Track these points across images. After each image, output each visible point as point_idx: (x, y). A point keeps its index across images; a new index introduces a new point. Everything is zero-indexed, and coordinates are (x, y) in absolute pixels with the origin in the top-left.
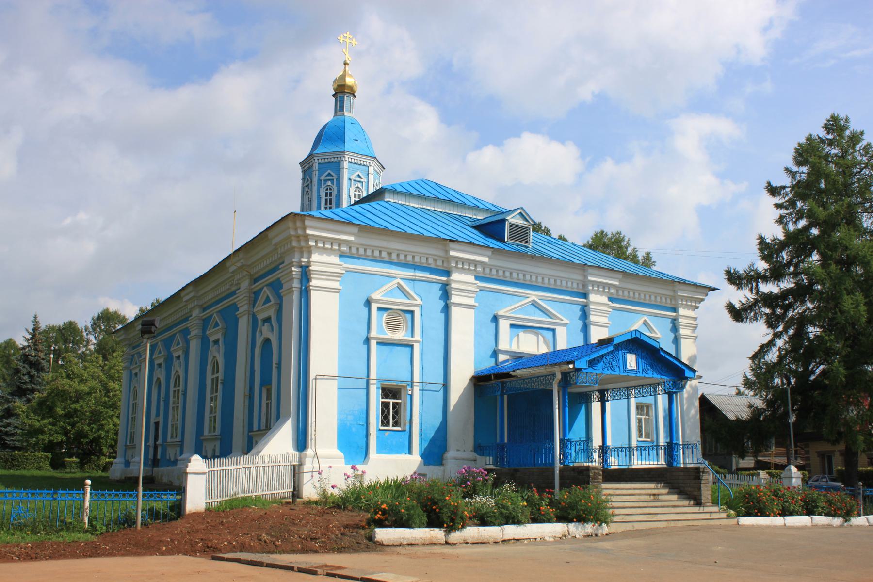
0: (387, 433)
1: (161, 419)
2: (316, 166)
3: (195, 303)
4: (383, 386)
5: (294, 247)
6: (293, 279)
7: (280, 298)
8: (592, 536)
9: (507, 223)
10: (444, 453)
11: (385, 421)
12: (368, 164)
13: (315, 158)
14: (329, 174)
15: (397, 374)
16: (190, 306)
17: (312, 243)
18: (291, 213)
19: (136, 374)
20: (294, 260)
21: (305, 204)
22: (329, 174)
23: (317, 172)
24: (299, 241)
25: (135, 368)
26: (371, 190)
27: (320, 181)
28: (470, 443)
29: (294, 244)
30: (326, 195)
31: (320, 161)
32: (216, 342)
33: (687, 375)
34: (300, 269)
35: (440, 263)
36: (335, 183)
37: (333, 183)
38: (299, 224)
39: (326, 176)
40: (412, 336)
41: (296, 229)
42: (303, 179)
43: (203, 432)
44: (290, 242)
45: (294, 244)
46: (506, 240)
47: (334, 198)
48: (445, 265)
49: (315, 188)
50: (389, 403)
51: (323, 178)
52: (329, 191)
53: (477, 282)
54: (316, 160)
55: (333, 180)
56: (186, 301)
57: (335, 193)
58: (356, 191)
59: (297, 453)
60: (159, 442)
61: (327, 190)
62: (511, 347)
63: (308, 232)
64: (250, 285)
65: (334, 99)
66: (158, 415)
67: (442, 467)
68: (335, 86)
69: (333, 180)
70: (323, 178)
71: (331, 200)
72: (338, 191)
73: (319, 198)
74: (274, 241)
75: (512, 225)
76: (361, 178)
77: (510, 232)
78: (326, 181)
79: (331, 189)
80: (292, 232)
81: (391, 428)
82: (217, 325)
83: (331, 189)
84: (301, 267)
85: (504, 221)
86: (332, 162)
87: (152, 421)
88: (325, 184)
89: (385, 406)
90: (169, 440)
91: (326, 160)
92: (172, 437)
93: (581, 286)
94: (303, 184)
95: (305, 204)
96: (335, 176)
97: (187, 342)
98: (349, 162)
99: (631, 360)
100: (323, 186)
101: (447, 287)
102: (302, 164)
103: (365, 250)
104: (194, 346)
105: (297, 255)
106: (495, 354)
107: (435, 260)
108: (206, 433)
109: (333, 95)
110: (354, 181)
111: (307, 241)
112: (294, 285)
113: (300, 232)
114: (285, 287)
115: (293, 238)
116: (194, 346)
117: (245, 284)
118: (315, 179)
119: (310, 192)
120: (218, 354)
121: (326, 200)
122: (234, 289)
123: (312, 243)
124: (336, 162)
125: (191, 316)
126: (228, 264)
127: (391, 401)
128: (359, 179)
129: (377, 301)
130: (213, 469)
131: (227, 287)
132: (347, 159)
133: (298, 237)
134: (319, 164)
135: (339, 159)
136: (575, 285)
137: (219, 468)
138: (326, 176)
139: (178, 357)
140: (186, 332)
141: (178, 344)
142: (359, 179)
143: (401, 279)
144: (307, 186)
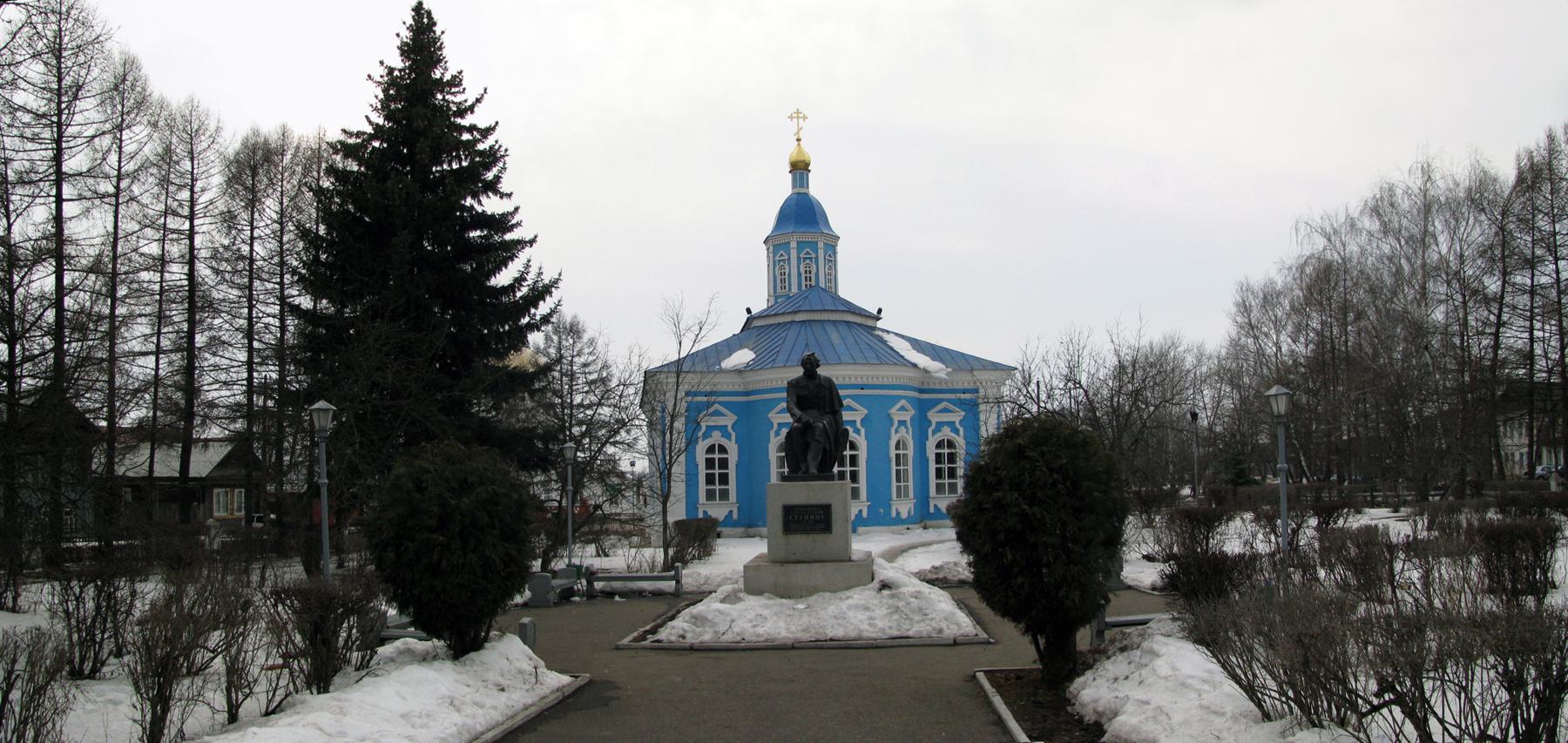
14: (782, 255)
22: (782, 255)
51: (777, 258)
70: (777, 258)
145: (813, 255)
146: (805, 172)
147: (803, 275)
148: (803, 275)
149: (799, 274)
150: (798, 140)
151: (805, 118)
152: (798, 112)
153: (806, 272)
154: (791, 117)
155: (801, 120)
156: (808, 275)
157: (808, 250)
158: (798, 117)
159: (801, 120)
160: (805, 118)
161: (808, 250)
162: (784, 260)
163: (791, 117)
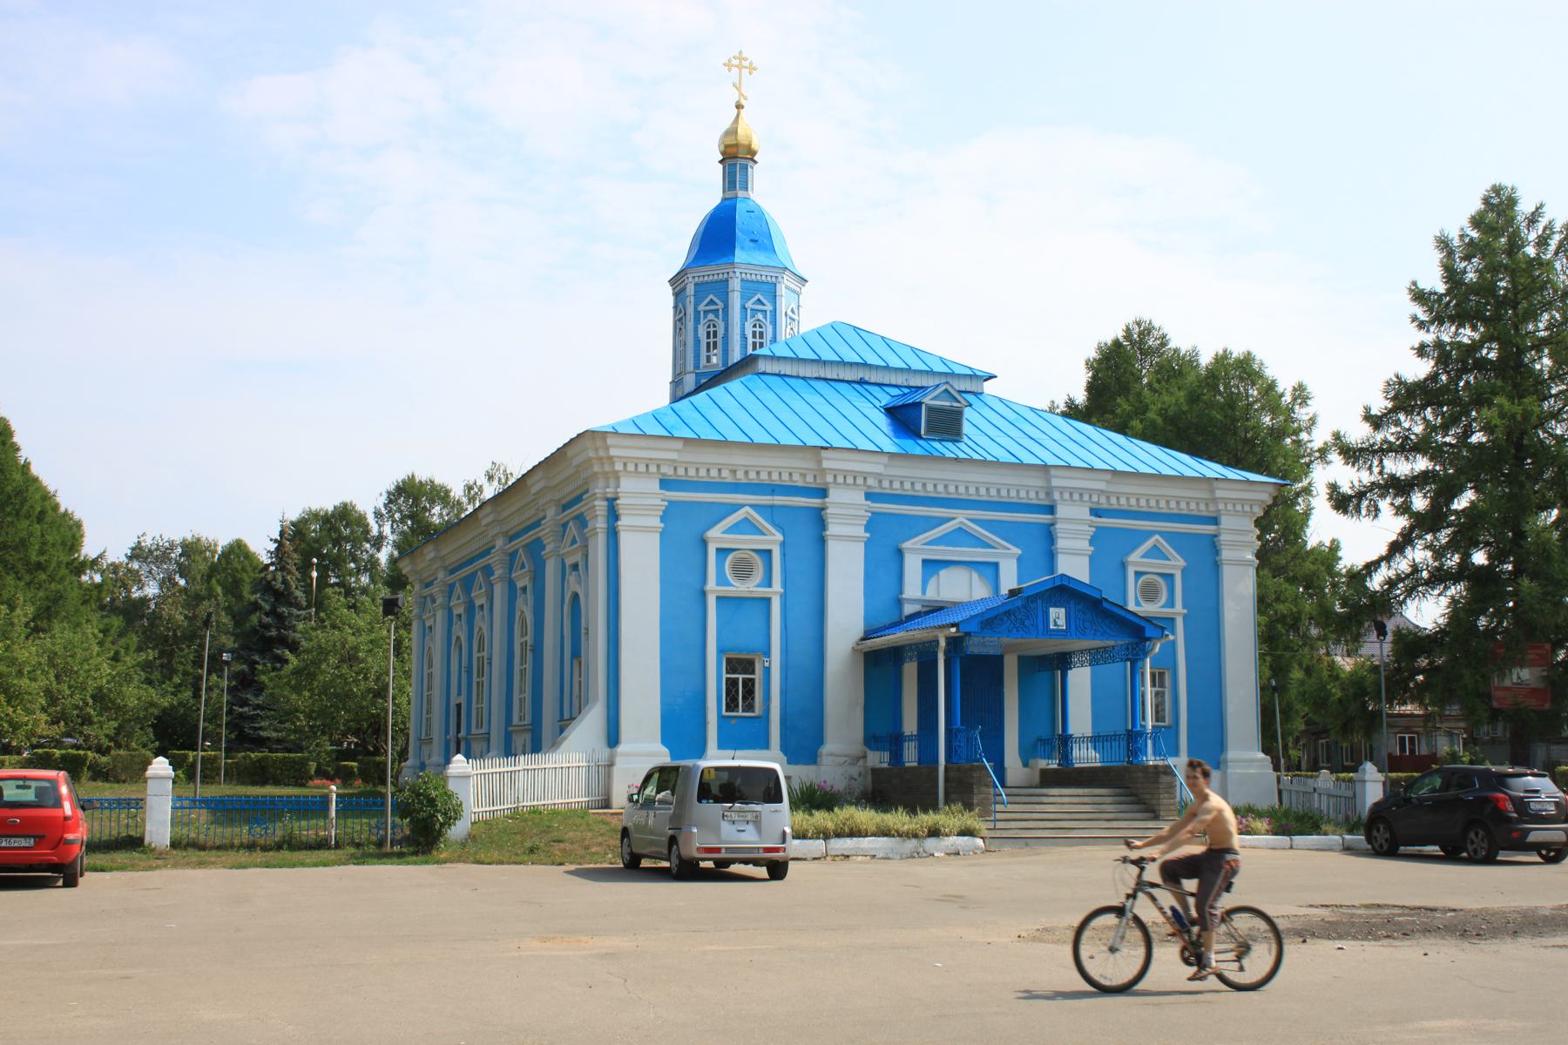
0: (733, 722)
1: (463, 700)
2: (691, 289)
3: (497, 530)
4: (732, 655)
5: (596, 474)
6: (597, 516)
7: (586, 540)
8: (958, 854)
9: (924, 407)
10: (819, 747)
11: (732, 704)
12: (774, 279)
13: (689, 275)
14: (712, 302)
15: (744, 643)
16: (491, 534)
17: (619, 467)
18: (587, 431)
19: (430, 628)
20: (596, 491)
21: (679, 349)
22: (712, 302)
23: (692, 298)
24: (602, 464)
25: (428, 618)
26: (736, 356)
27: (697, 313)
28: (859, 733)
29: (596, 469)
30: (708, 337)
31: (696, 279)
32: (524, 589)
33: (1148, 634)
34: (605, 503)
35: (810, 479)
36: (721, 317)
37: (717, 316)
38: (599, 443)
39: (706, 306)
40: (770, 585)
41: (597, 450)
42: (675, 307)
43: (511, 721)
44: (592, 465)
45: (596, 469)
46: (923, 432)
47: (719, 339)
48: (818, 481)
49: (690, 325)
50: (738, 679)
51: (702, 308)
52: (712, 329)
53: (869, 503)
54: (690, 279)
55: (718, 310)
56: (487, 525)
57: (721, 333)
58: (755, 326)
59: (608, 749)
60: (463, 733)
61: (709, 327)
62: (924, 592)
63: (613, 452)
64: (556, 515)
65: (721, 166)
66: (459, 694)
67: (813, 768)
68: (722, 148)
69: (718, 310)
71: (715, 343)
72: (726, 329)
73: (697, 341)
74: (576, 461)
75: (930, 409)
76: (763, 304)
77: (928, 422)
78: (706, 312)
79: (714, 326)
80: (592, 454)
81: (740, 713)
82: (523, 566)
83: (714, 326)
84: (607, 499)
85: (920, 404)
86: (716, 282)
87: (453, 702)
88: (705, 317)
89: (732, 684)
90: (474, 731)
91: (706, 278)
92: (477, 727)
93: (1042, 495)
94: (675, 316)
95: (679, 349)
96: (720, 305)
97: (491, 586)
98: (742, 280)
99: (1058, 616)
100: (702, 322)
101: (823, 513)
102: (672, 282)
103: (697, 470)
104: (499, 591)
105: (601, 483)
106: (899, 602)
107: (804, 476)
108: (515, 720)
109: (721, 162)
110: (751, 310)
111: (613, 464)
112: (598, 526)
113: (602, 453)
114: (590, 525)
115: (594, 461)
116: (499, 591)
117: (551, 512)
118: (690, 310)
119: (683, 330)
120: (525, 607)
121: (708, 344)
122: (541, 515)
123: (619, 467)
124: (721, 281)
125: (493, 547)
126: (529, 481)
127: (741, 677)
128: (760, 307)
129: (716, 539)
130: (483, 771)
131: (533, 511)
132: (738, 274)
133: (601, 459)
134: (695, 285)
135: (725, 276)
136: (1032, 495)
137: (491, 770)
138: (706, 306)
139: (482, 607)
140: (488, 571)
141: (481, 588)
142: (760, 307)
143: (751, 506)
144: (680, 320)
145: (769, 307)
146: (751, 163)
147: (750, 340)
148: (750, 340)
149: (744, 337)
150: (739, 106)
151: (752, 69)
152: (740, 57)
153: (754, 336)
154: (729, 65)
155: (745, 72)
156: (758, 340)
157: (759, 296)
158: (740, 67)
159: (745, 72)
160: (752, 69)
161: (711, 296)
162: (715, 312)
163: (729, 65)
